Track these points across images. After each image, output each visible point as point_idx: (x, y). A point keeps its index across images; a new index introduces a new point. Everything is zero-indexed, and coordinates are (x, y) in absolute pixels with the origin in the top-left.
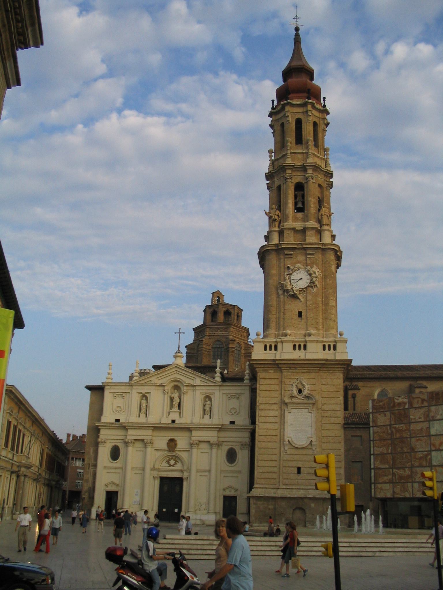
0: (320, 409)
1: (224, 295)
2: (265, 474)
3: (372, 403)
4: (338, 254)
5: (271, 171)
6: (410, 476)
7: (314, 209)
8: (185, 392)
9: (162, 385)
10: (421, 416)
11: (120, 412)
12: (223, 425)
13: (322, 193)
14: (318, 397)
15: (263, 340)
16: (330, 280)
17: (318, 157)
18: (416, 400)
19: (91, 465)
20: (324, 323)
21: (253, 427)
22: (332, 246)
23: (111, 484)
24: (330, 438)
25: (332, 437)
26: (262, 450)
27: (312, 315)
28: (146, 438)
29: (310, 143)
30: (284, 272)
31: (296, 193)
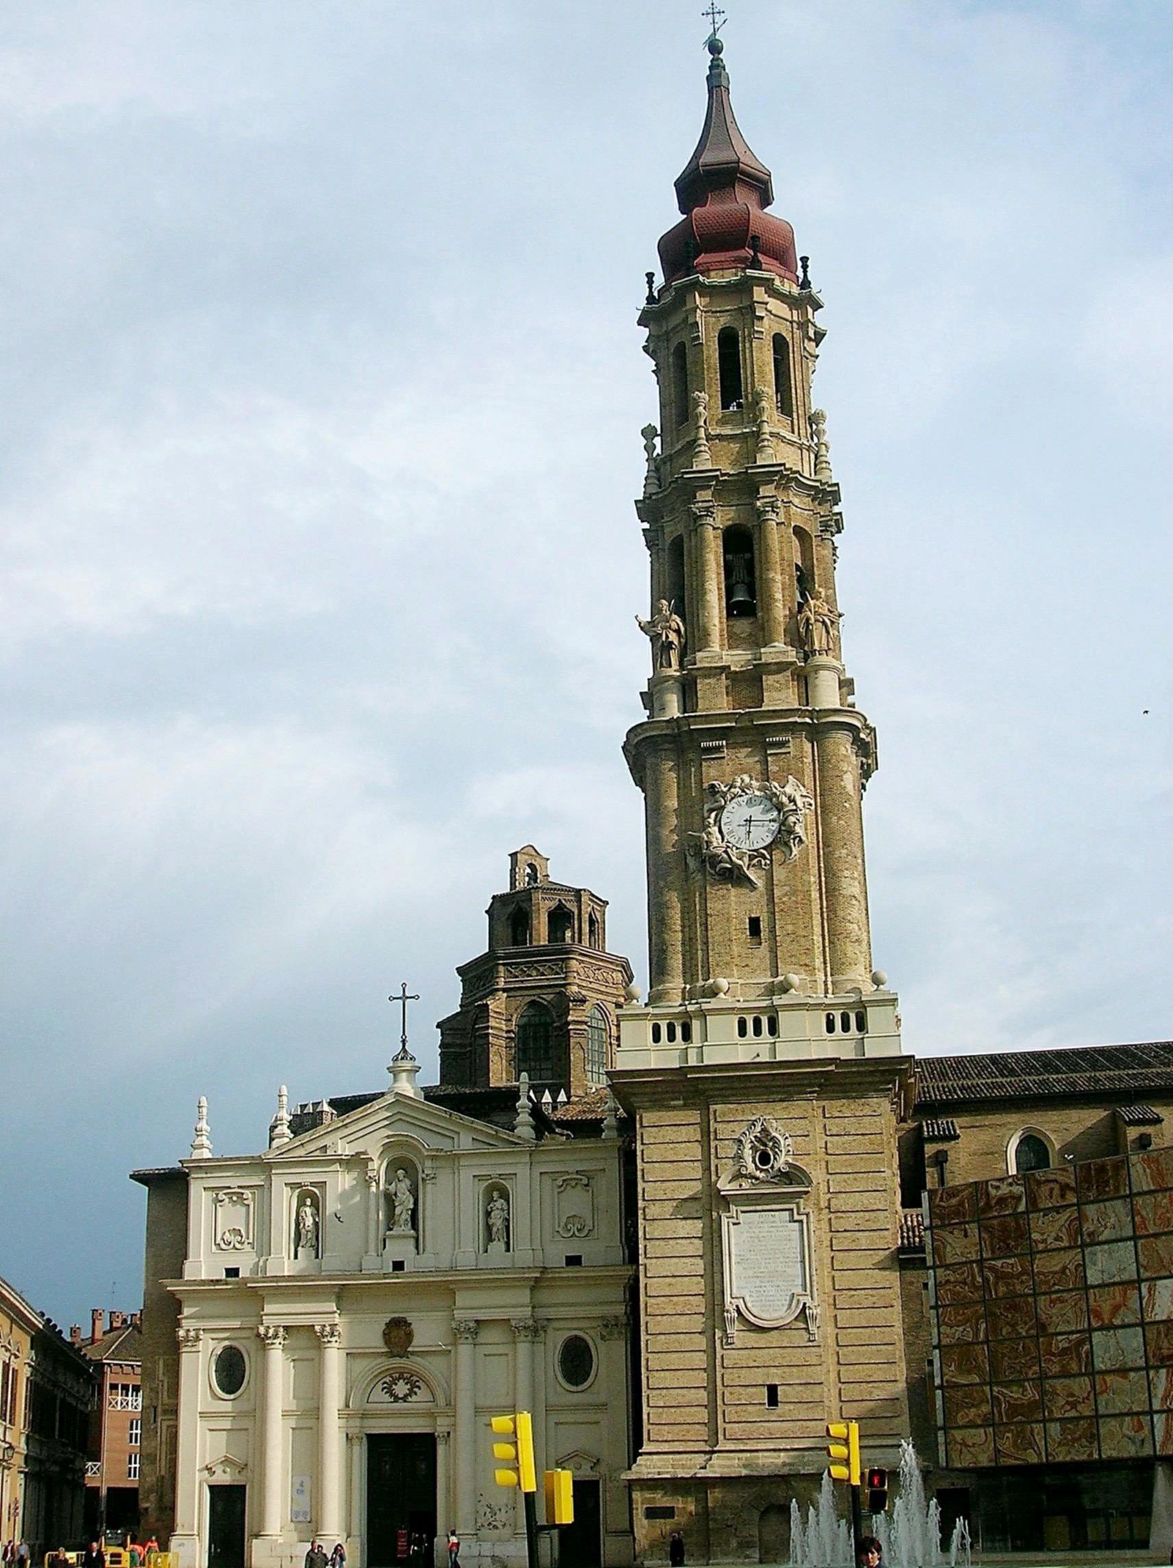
0: (826, 1208)
1: (548, 859)
3: (930, 1199)
4: (862, 736)
5: (651, 495)
6: (1039, 1405)
7: (784, 605)
8: (427, 1175)
10: (1060, 1235)
11: (238, 1246)
12: (544, 1269)
13: (806, 551)
14: (817, 1175)
15: (650, 1010)
16: (839, 818)
17: (791, 443)
18: (1045, 1189)
19: (159, 1410)
20: (827, 949)
22: (839, 715)
26: (663, 1337)
27: (790, 928)
28: (317, 1322)
29: (764, 403)
30: (703, 803)
31: (730, 557)
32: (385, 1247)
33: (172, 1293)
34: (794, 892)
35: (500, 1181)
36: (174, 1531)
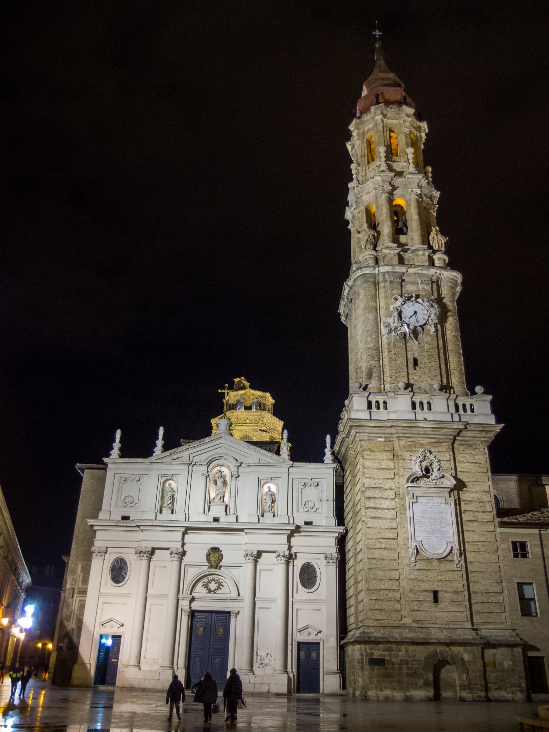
2: (381, 602)
21: (344, 530)
24: (480, 543)
25: (483, 543)
26: (374, 561)
32: (209, 510)
33: (92, 526)
34: (433, 348)
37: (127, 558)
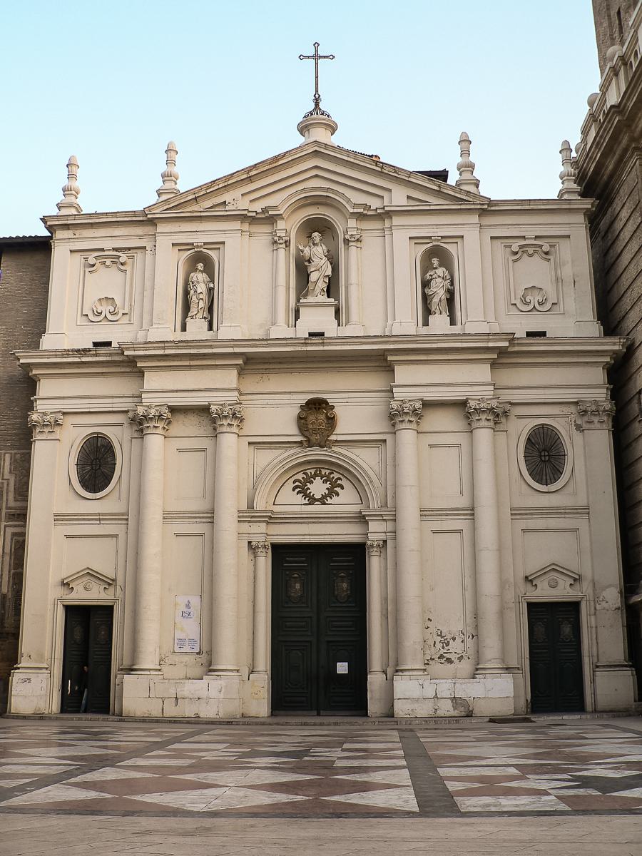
8: (351, 236)
9: (269, 218)
11: (110, 317)
12: (512, 339)
23: (88, 577)
28: (216, 400)
32: (297, 317)
35: (442, 245)
36: (16, 663)
37: (113, 434)
